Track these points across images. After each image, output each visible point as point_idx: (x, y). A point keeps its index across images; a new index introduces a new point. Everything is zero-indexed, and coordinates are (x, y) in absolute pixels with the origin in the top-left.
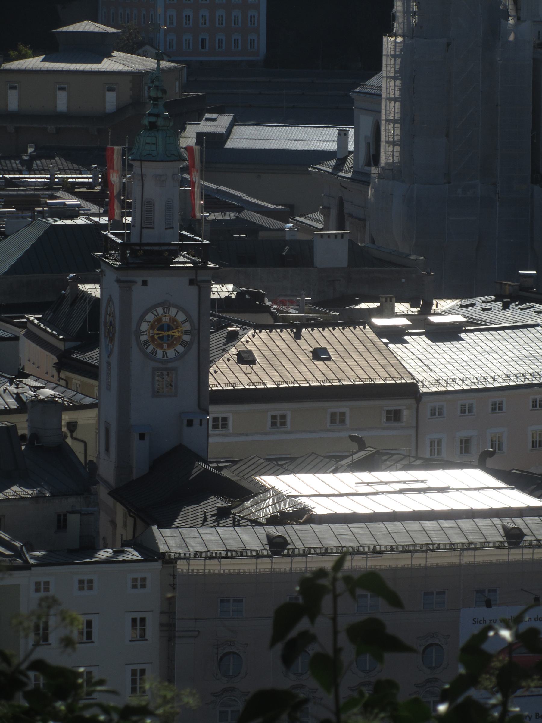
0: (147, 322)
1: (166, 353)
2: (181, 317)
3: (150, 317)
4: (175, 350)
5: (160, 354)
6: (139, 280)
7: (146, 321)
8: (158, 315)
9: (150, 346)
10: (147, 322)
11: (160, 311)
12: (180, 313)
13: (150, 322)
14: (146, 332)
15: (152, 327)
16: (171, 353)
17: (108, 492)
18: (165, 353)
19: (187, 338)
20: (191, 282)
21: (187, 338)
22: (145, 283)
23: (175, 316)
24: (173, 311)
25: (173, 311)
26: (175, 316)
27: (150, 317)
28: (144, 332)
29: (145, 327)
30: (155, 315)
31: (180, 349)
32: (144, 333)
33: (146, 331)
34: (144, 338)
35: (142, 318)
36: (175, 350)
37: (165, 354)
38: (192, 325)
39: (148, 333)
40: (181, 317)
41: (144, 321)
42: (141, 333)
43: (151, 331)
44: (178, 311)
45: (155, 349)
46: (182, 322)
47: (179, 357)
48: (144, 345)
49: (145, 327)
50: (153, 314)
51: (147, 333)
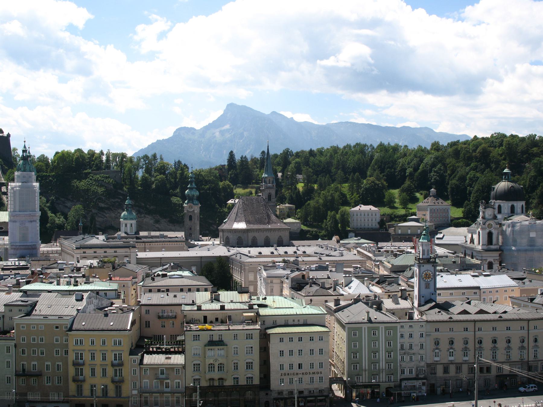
5: (426, 280)
6: (422, 265)
11: (426, 272)
15: (425, 275)
16: (429, 280)
19: (432, 277)
20: (433, 266)
21: (432, 277)
22: (423, 266)
24: (429, 272)
25: (429, 272)
27: (424, 273)
29: (423, 275)
31: (430, 279)
34: (423, 277)
35: (423, 273)
40: (431, 273)
47: (431, 281)
49: (423, 275)
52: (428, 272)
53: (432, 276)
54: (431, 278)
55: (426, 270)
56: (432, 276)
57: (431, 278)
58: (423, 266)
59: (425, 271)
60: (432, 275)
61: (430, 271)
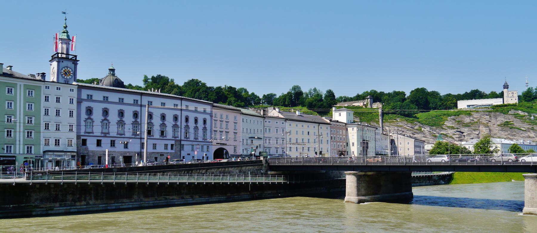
2: (70, 70)
3: (64, 69)
5: (66, 77)
6: (61, 61)
11: (66, 68)
15: (64, 71)
16: (68, 78)
19: (72, 75)
20: (73, 63)
21: (72, 75)
22: (63, 62)
24: (69, 69)
27: (64, 69)
34: (62, 73)
35: (62, 69)
37: (67, 77)
38: (73, 72)
40: (70, 70)
52: (67, 69)
53: (72, 74)
54: (71, 76)
55: (66, 66)
56: (72, 74)
57: (71, 76)
58: (63, 62)
59: (64, 68)
60: (72, 72)
61: (70, 68)
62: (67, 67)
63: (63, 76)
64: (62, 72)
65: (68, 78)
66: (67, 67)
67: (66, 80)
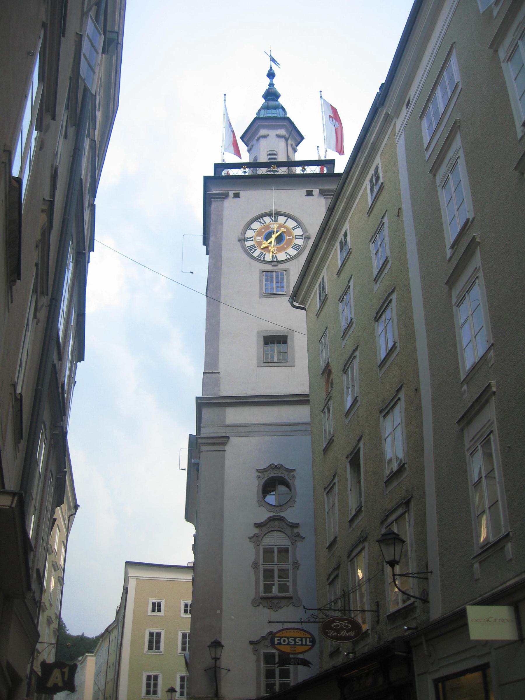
0: (253, 229)
1: (276, 256)
2: (291, 224)
3: (256, 225)
4: (286, 253)
7: (252, 229)
8: (266, 223)
9: (257, 250)
10: (253, 229)
11: (267, 219)
12: (290, 220)
13: (256, 230)
14: (252, 238)
15: (259, 234)
17: (200, 395)
18: (274, 256)
21: (300, 242)
23: (285, 223)
25: (281, 219)
26: (285, 223)
28: (250, 238)
30: (261, 223)
32: (250, 239)
33: (253, 237)
34: (248, 244)
36: (286, 253)
39: (255, 239)
41: (249, 229)
42: (246, 239)
43: (257, 237)
44: (287, 219)
45: (263, 253)
46: (292, 228)
48: (250, 250)
49: (250, 233)
50: (260, 222)
51: (253, 239)
53: (298, 237)
54: (296, 247)
55: (268, 210)
56: (298, 237)
57: (296, 247)
60: (299, 232)
61: (288, 216)
62: (269, 214)
63: (256, 254)
64: (247, 240)
65: (282, 256)
66: (275, 214)
67: (269, 267)
